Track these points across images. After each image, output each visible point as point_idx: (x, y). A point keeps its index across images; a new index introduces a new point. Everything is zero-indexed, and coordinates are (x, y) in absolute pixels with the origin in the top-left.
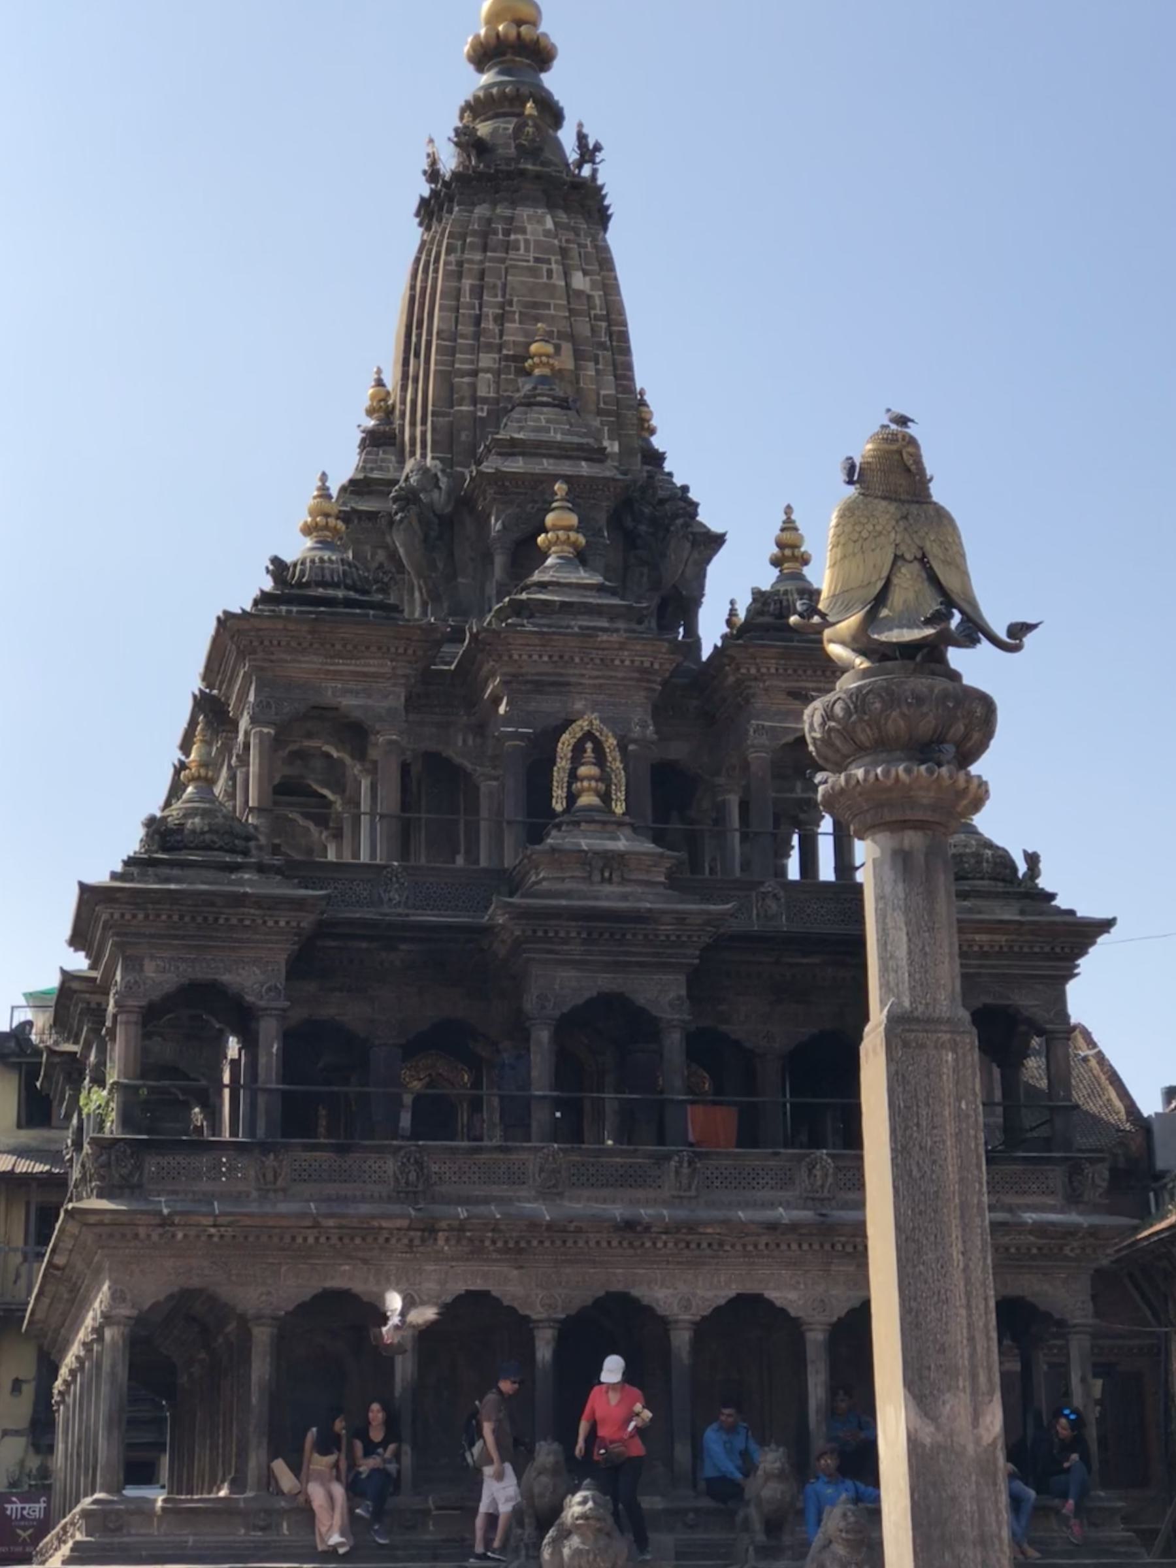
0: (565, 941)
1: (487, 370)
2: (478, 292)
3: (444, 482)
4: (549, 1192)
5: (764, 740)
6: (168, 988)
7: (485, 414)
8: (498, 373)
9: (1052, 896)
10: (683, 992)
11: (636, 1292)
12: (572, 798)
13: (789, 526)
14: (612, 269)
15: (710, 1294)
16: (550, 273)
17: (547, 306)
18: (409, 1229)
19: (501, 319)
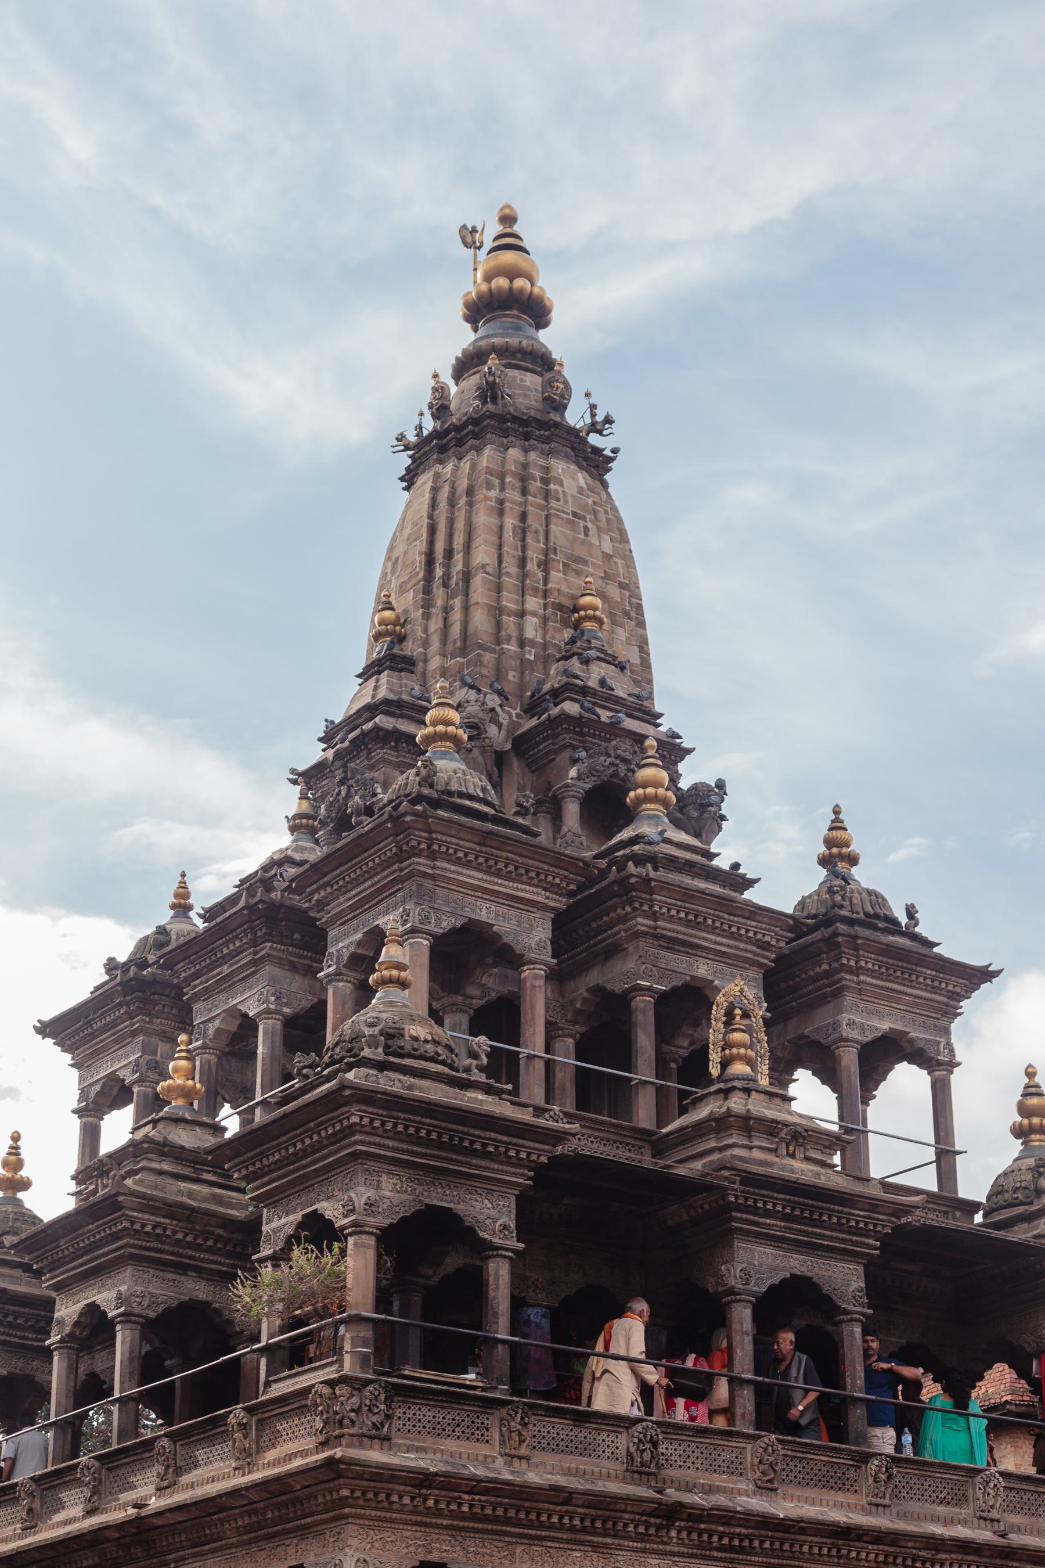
0: (767, 1214)
1: (534, 614)
2: (523, 532)
3: (503, 719)
4: (766, 1488)
5: (855, 1034)
6: (405, 1212)
7: (532, 658)
8: (545, 620)
10: (863, 1285)
12: (725, 1064)
13: (837, 825)
14: (627, 542)
16: (586, 530)
17: (585, 562)
18: (651, 1515)
19: (545, 565)
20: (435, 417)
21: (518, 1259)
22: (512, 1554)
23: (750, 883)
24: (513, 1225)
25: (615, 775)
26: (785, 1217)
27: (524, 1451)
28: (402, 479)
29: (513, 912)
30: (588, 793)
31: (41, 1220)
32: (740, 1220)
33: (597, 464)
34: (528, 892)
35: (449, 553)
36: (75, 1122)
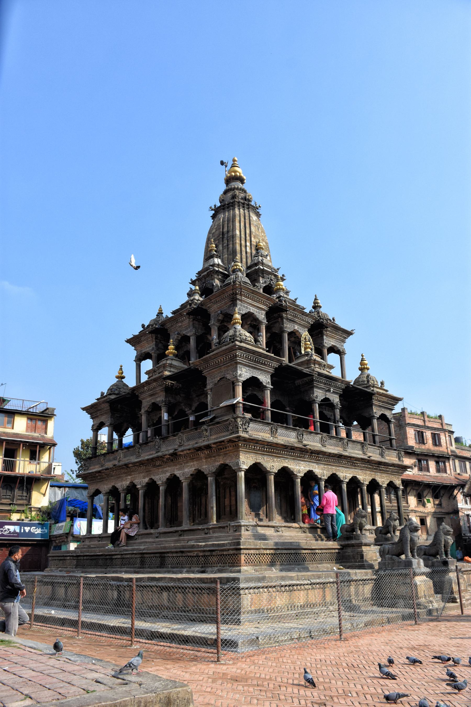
0: (321, 382)
9: (387, 391)
11: (337, 474)
15: (349, 475)
20: (221, 202)
21: (272, 391)
22: (274, 461)
23: (304, 309)
24: (270, 382)
25: (270, 283)
26: (325, 384)
27: (276, 436)
28: (211, 217)
29: (258, 311)
30: (264, 287)
31: (127, 386)
32: (315, 384)
33: (258, 215)
34: (261, 306)
35: (228, 232)
36: (135, 363)
